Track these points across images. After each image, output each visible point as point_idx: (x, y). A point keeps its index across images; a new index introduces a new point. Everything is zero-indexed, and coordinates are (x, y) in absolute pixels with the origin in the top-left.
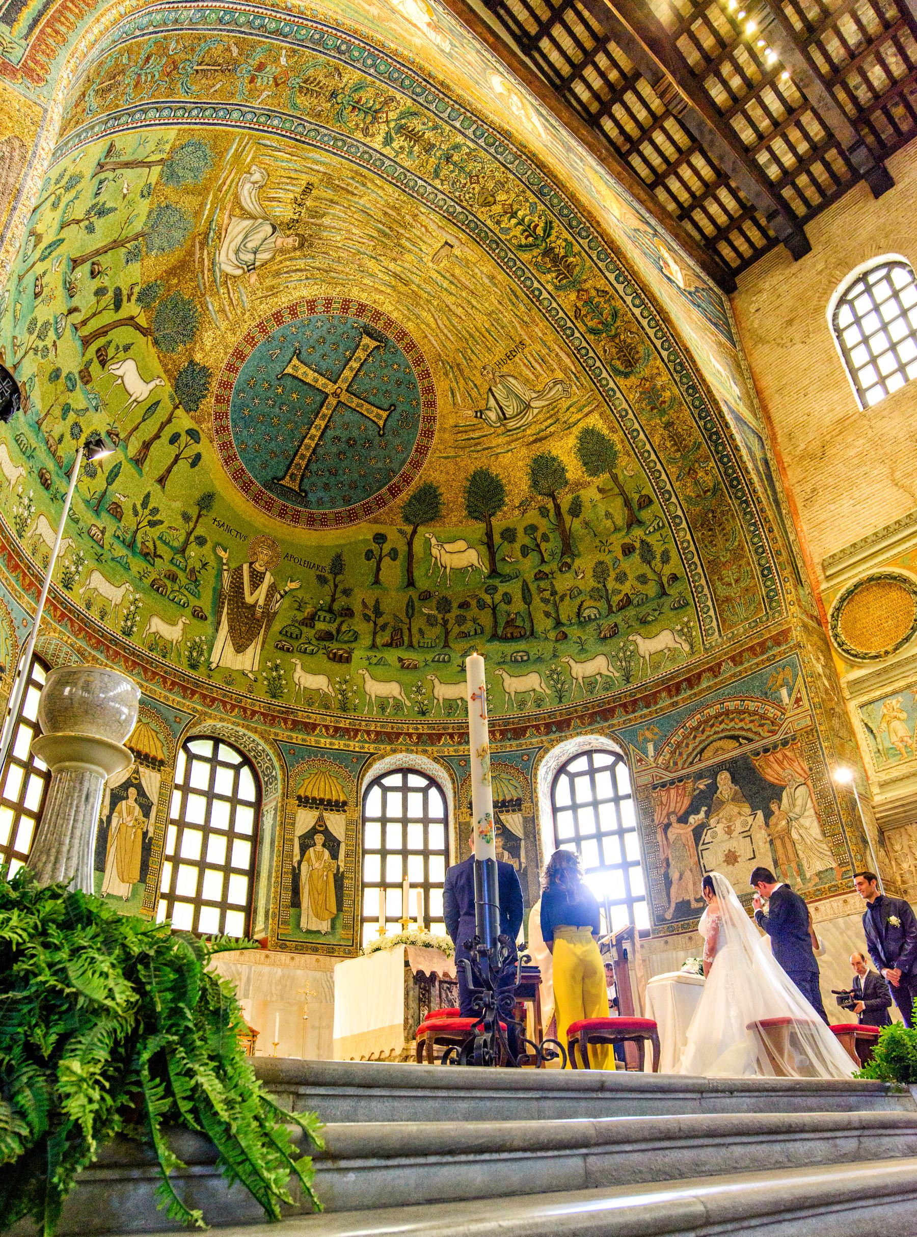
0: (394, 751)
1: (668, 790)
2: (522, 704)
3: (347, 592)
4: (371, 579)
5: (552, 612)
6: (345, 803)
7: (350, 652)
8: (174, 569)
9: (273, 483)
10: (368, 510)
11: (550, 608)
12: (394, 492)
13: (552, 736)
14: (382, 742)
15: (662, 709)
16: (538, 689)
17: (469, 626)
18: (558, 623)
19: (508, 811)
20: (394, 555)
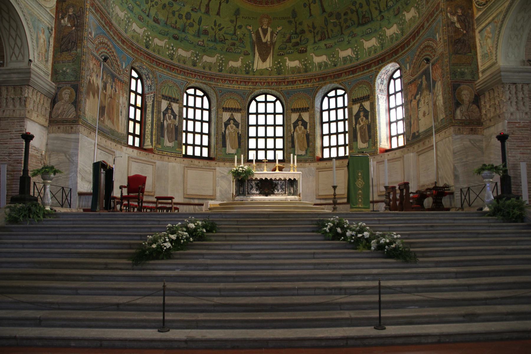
0: (325, 84)
1: (412, 85)
3: (301, 24)
4: (309, 14)
5: (378, 7)
6: (308, 108)
7: (306, 48)
8: (234, 41)
11: (377, 5)
13: (380, 65)
14: (321, 81)
15: (411, 47)
16: (375, 45)
18: (381, 12)
19: (365, 101)
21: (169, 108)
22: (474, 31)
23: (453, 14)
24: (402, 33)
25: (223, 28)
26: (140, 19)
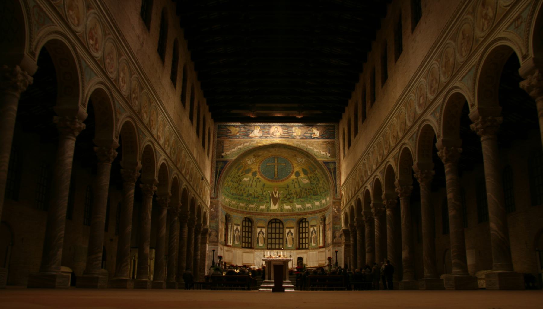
2: (317, 207)
3: (291, 190)
4: (294, 187)
7: (293, 200)
8: (262, 197)
9: (273, 178)
10: (290, 177)
12: (292, 173)
17: (310, 193)
18: (320, 193)
20: (296, 182)
21: (237, 228)
22: (341, 213)
23: (335, 208)
24: (326, 204)
25: (258, 192)
26: (228, 196)
